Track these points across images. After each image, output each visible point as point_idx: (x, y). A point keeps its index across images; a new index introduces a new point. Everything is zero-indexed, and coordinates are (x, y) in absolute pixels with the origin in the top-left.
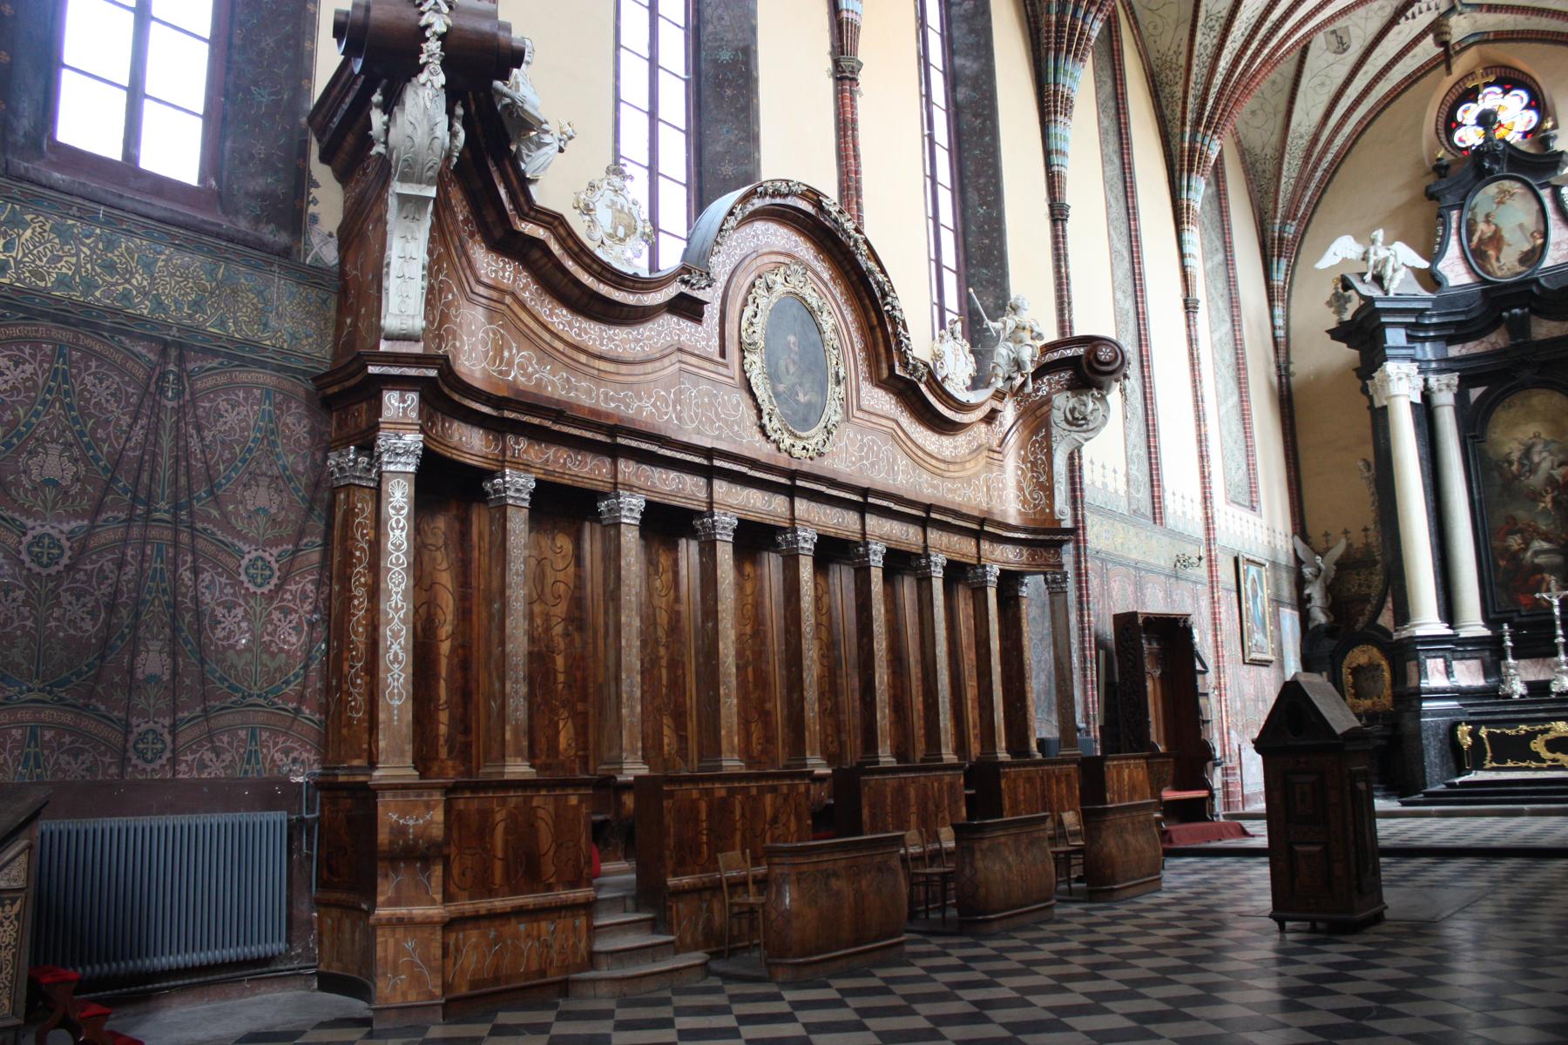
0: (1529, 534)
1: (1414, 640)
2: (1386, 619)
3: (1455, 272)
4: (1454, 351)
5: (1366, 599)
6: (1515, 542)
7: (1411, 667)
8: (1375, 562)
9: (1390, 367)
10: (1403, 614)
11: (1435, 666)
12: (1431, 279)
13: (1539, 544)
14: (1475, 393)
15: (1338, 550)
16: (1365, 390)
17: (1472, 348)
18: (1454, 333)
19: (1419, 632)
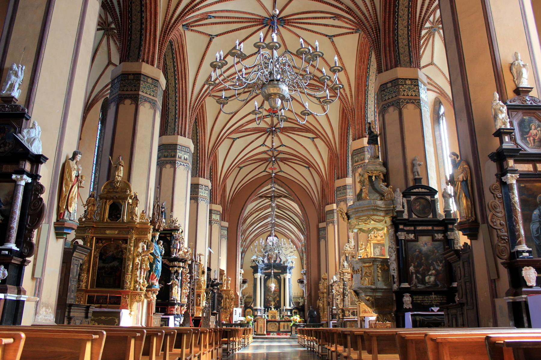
0: (270, 296)
1: (257, 309)
2: (252, 306)
3: (266, 261)
4: (264, 271)
5: (250, 302)
6: (268, 297)
7: (256, 312)
8: (251, 298)
9: (258, 274)
10: (255, 305)
11: (259, 312)
12: (263, 261)
13: (271, 298)
14: (266, 277)
15: (246, 296)
16: (254, 275)
17: (267, 271)
18: (266, 269)
19: (258, 308)
